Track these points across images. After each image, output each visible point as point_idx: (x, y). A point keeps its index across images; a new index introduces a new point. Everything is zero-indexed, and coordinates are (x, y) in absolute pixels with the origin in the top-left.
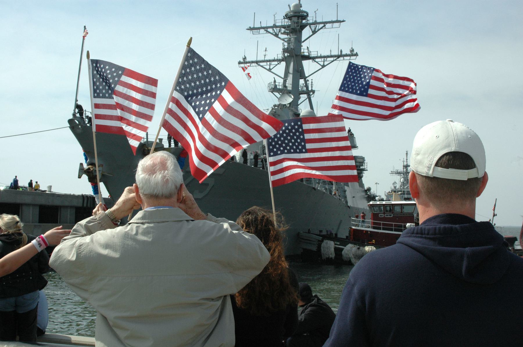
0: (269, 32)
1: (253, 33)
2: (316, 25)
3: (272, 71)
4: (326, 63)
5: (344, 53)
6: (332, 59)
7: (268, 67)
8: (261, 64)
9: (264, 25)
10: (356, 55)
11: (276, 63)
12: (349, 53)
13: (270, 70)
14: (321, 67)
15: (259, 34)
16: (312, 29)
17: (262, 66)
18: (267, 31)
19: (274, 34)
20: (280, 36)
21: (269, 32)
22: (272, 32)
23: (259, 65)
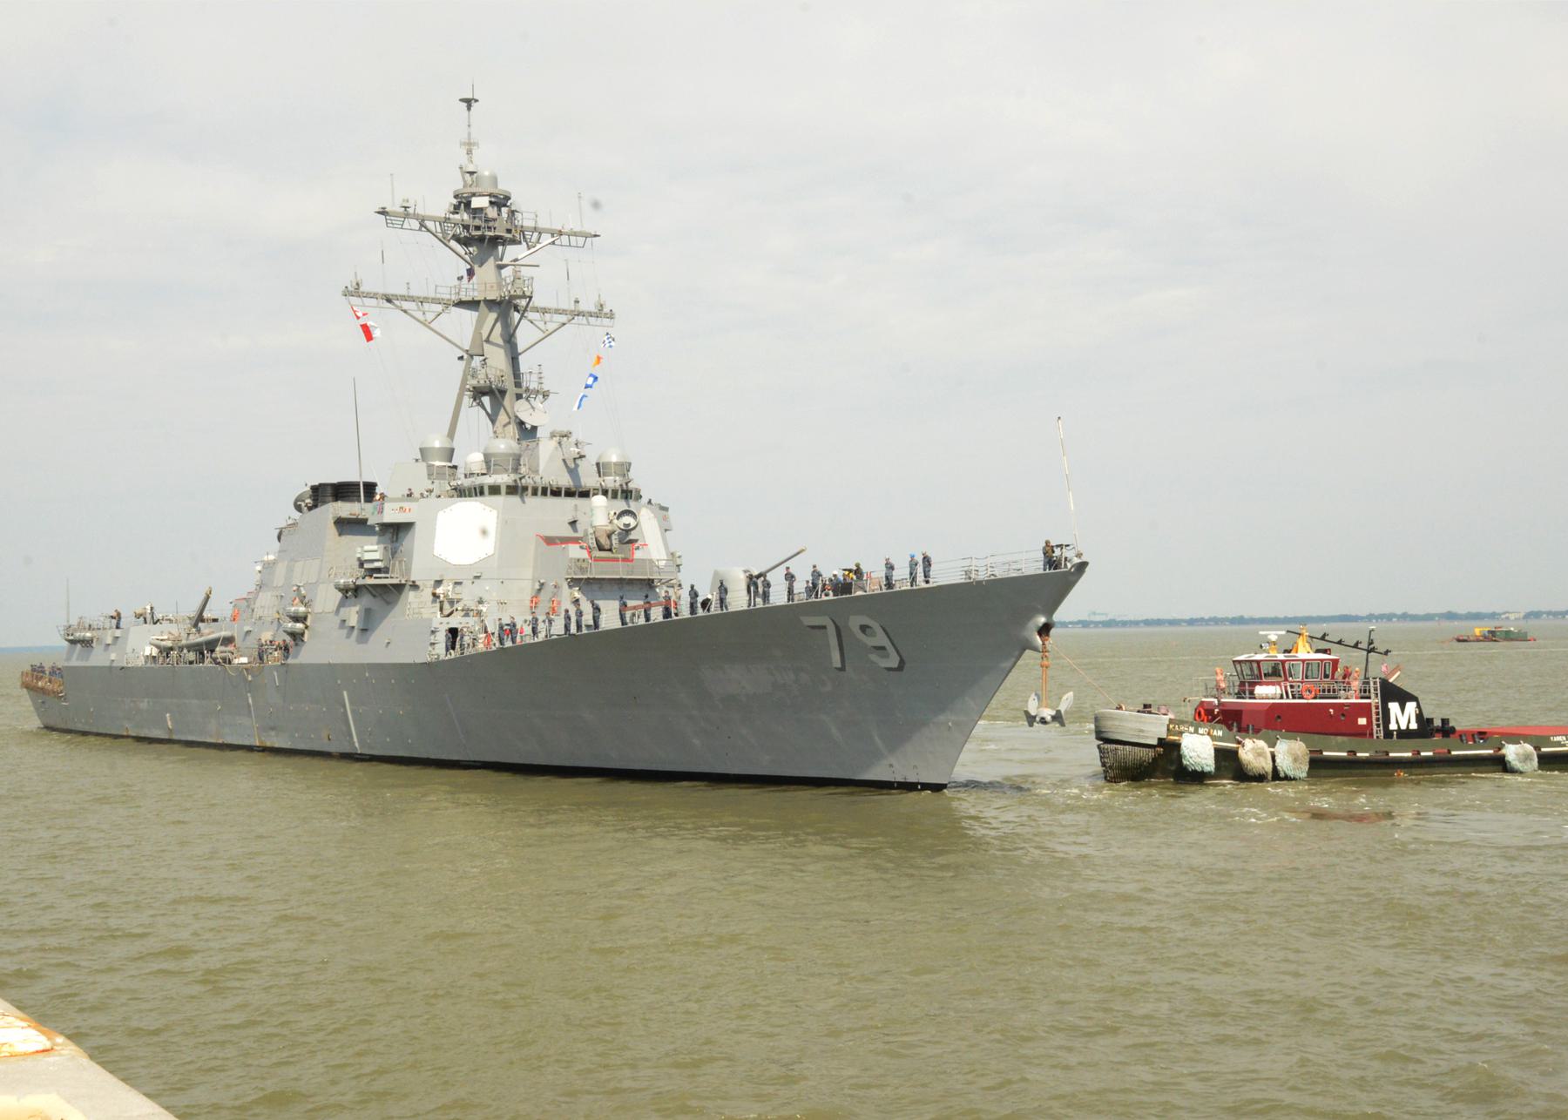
0: (428, 230)
1: (387, 223)
2: (536, 234)
3: (432, 325)
4: (551, 327)
5: (582, 307)
6: (563, 318)
7: (419, 315)
8: (406, 305)
9: (420, 211)
10: (611, 316)
11: (439, 308)
12: (593, 309)
13: (426, 324)
14: (542, 335)
15: (402, 228)
16: (527, 237)
17: (405, 311)
18: (422, 225)
19: (440, 235)
20: (453, 244)
21: (428, 230)
22: (433, 230)
23: (397, 307)
